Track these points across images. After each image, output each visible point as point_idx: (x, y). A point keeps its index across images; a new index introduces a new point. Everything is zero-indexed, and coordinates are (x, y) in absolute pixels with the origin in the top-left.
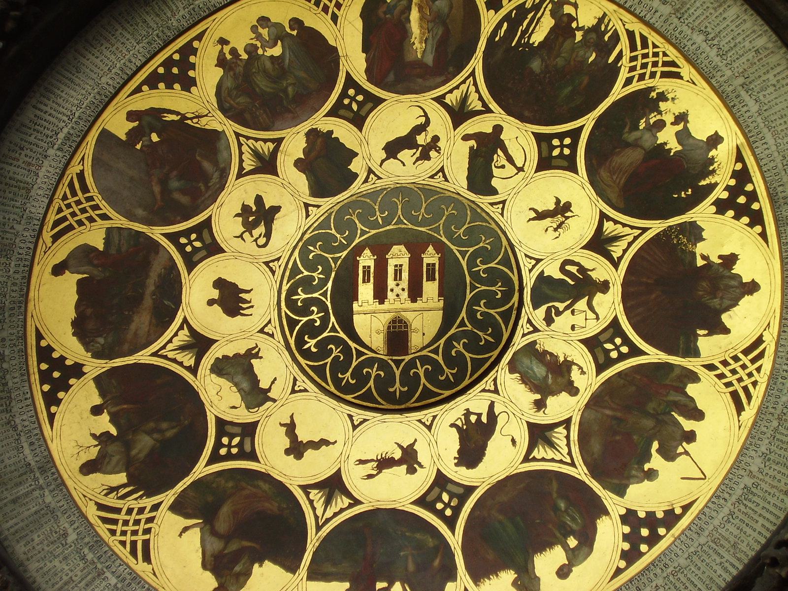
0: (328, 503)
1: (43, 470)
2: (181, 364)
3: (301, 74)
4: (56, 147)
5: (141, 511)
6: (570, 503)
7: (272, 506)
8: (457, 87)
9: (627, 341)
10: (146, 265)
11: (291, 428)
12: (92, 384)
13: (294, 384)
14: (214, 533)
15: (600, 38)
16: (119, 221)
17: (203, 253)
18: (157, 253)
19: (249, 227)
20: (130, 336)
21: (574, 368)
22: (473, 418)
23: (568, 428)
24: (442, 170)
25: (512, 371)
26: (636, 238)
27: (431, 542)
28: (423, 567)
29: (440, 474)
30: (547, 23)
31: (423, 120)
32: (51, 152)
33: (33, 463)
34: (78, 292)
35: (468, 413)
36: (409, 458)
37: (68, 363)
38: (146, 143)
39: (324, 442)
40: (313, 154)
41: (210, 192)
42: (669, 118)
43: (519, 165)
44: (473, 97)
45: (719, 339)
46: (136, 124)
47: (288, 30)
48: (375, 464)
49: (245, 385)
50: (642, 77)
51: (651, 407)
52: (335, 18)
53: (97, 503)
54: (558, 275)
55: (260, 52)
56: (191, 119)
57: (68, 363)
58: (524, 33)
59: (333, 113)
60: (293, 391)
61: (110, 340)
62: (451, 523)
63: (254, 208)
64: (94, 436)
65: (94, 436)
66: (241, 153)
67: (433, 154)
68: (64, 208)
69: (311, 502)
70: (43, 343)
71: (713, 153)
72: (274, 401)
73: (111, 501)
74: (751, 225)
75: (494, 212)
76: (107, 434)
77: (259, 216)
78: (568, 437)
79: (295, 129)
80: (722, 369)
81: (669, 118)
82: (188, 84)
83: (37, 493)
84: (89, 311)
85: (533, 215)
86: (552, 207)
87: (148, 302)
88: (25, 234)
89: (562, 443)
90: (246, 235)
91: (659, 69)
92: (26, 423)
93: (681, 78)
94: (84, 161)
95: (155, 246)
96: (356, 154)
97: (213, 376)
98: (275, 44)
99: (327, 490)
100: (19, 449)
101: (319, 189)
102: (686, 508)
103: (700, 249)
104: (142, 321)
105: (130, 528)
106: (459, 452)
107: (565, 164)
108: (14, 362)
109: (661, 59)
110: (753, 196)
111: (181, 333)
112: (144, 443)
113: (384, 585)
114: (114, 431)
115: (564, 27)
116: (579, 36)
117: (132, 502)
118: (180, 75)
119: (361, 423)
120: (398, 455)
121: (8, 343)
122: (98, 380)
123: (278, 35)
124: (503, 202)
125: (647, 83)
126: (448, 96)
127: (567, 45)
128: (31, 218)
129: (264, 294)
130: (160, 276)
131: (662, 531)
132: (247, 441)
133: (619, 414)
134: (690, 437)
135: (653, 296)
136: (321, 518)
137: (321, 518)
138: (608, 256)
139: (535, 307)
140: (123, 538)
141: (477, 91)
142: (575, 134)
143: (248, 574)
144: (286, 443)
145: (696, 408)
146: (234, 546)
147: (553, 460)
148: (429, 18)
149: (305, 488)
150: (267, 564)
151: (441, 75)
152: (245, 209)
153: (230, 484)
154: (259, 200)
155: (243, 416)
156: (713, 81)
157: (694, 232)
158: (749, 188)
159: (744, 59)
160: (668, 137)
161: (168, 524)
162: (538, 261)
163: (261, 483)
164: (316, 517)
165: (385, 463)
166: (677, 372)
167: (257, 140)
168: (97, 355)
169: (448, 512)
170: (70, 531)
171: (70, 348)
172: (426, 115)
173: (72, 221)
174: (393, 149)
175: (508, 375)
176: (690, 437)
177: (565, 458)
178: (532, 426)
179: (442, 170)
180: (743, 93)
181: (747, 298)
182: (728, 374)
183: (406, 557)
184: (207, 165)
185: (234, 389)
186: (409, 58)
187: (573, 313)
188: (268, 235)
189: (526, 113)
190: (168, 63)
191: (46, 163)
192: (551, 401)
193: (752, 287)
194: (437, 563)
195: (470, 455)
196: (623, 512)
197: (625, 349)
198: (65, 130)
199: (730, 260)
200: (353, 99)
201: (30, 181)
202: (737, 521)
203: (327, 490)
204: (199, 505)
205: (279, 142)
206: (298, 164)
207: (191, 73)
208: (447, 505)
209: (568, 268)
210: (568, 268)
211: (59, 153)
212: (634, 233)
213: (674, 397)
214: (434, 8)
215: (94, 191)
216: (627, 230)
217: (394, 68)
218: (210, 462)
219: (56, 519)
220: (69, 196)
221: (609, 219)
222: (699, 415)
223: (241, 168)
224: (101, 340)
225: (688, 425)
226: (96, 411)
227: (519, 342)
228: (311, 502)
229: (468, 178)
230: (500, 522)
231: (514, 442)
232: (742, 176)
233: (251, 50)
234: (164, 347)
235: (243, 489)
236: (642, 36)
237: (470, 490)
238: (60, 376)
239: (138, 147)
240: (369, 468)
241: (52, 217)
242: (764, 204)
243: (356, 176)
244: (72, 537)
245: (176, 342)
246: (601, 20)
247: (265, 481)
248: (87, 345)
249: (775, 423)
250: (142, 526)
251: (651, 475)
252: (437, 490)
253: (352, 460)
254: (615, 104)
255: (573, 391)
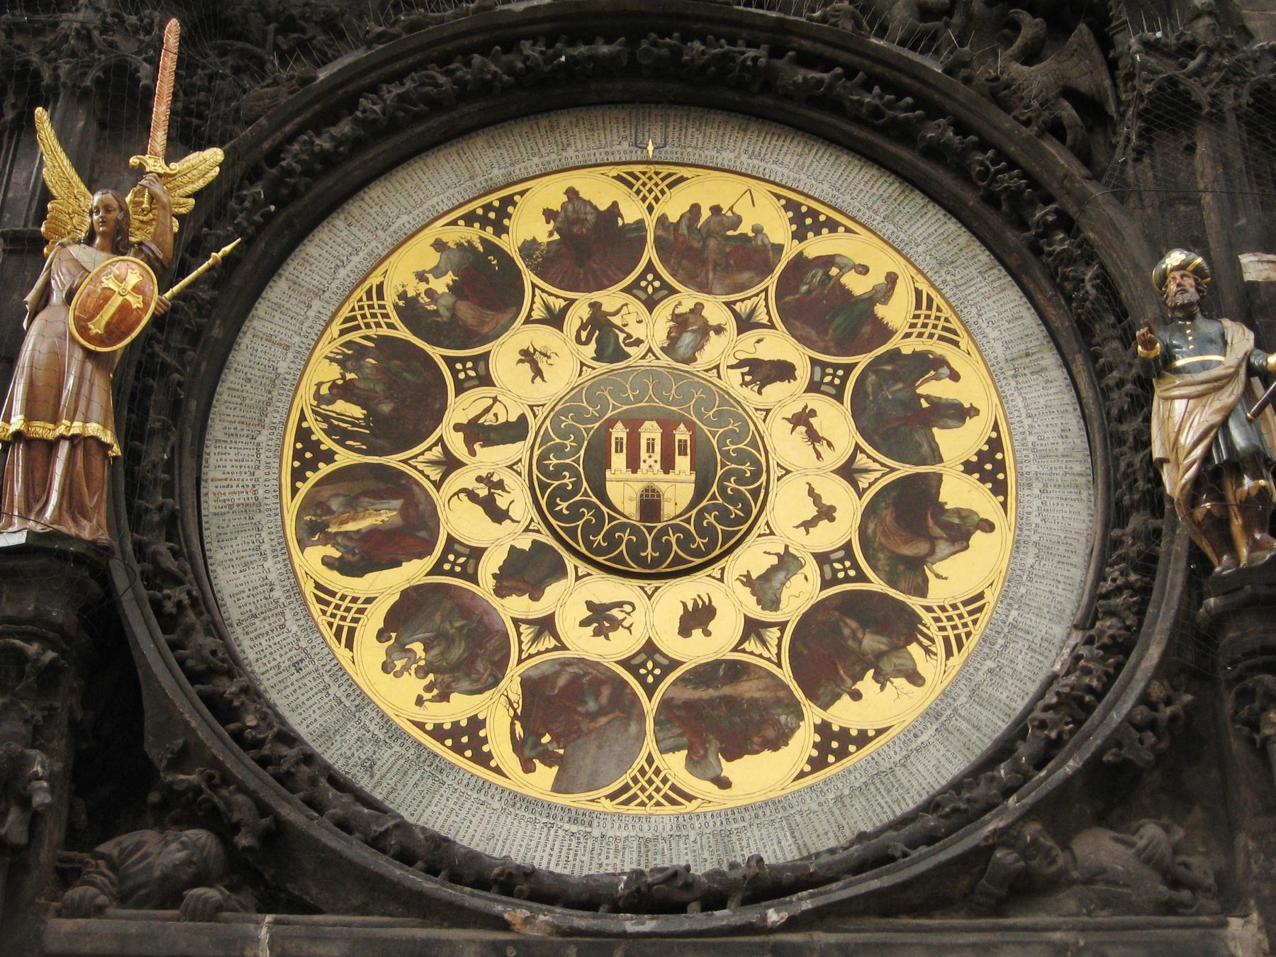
0: (867, 471)
1: (938, 716)
2: (780, 639)
3: (438, 618)
4: (589, 830)
5: (937, 620)
6: (802, 282)
7: (888, 515)
8: (422, 472)
9: (642, 276)
10: (688, 705)
11: (808, 525)
12: (832, 710)
13: (764, 535)
14: (932, 552)
15: (351, 357)
16: (650, 745)
17: (658, 657)
18: (672, 699)
19: (616, 624)
20: (769, 695)
21: (677, 312)
22: (748, 378)
23: (735, 302)
24: (511, 467)
25: (695, 360)
26: (543, 291)
27: (872, 378)
28: (895, 377)
29: (807, 391)
30: (341, 406)
31: (462, 495)
32: (596, 832)
33: (935, 727)
34: (740, 756)
35: (744, 384)
36: (802, 419)
37: (818, 739)
38: (555, 745)
39: (811, 492)
40: (522, 586)
41: (590, 670)
42: (423, 287)
43: (491, 401)
44: (428, 456)
45: (623, 209)
46: (536, 761)
47: (392, 642)
48: (817, 445)
49: (781, 576)
50: (385, 316)
51: (696, 245)
52: (369, 601)
53: (947, 658)
54: (593, 345)
55: (422, 663)
56: (515, 710)
57: (818, 739)
58: (353, 424)
59: (474, 579)
60: (772, 533)
61: (780, 711)
62: (849, 368)
63: (595, 625)
64: (882, 689)
65: (882, 689)
66: (539, 653)
67: (495, 478)
68: (654, 801)
69: (871, 485)
70: (808, 768)
71: (452, 245)
72: (787, 547)
73: (939, 647)
74: (515, 204)
75: (542, 414)
76: (875, 678)
77: (601, 618)
78: (742, 301)
79: (500, 610)
80: (650, 199)
81: (423, 287)
82: (476, 724)
83: (963, 712)
84: (756, 740)
85: (538, 379)
86: (527, 365)
87: (727, 690)
88: (697, 825)
89: (749, 303)
90: (626, 624)
91: (375, 302)
92: (897, 749)
93: (382, 283)
94: (593, 801)
95: (665, 704)
96: (512, 547)
97: (781, 606)
98: (411, 650)
99: (856, 476)
100: (925, 745)
101: (558, 571)
102: (779, 197)
103: (543, 238)
104: (748, 689)
105: (957, 621)
106: (782, 380)
107: (482, 364)
108: (840, 785)
109: (365, 303)
110: (488, 207)
111: (748, 649)
112: (871, 642)
113: (923, 401)
114: (871, 672)
115: (343, 391)
116: (350, 376)
117: (933, 631)
118: (468, 737)
119: (782, 468)
120: (802, 429)
121: (822, 799)
122: (825, 707)
123: (401, 648)
124: (531, 407)
125: (390, 310)
126: (432, 478)
127: (361, 385)
128: (678, 826)
129: (679, 594)
130: (695, 689)
131: (804, 209)
132: (833, 556)
133: (711, 267)
134: (716, 210)
135: (595, 266)
136: (882, 471)
137: (882, 471)
138: (565, 310)
139: (627, 356)
140: (970, 624)
141: (422, 453)
142: (450, 361)
143: (958, 511)
144: (824, 524)
145: (690, 211)
146: (937, 531)
147: (767, 306)
148: (352, 513)
149: (860, 494)
150: (941, 499)
151: (411, 490)
152: (597, 633)
153: (881, 556)
154: (585, 623)
155: (812, 568)
156: (383, 254)
157: (528, 248)
158: (480, 212)
159: (359, 234)
160: (441, 285)
161: (938, 592)
162: (582, 364)
163: (870, 531)
164: (883, 475)
165: (814, 437)
166: (660, 232)
167: (520, 642)
168: (800, 716)
169: (840, 373)
170: (985, 668)
171: (803, 742)
172: (457, 494)
173: (665, 789)
174: (498, 515)
175: (699, 360)
176: (716, 210)
177: (761, 297)
178: (741, 330)
179: (511, 467)
180: (392, 229)
181: (582, 195)
182: (653, 195)
183: (892, 393)
184: (562, 681)
185: (788, 584)
186: (398, 521)
187: (625, 325)
188: (619, 605)
189: (437, 406)
190: (458, 749)
191: (610, 833)
192: (713, 322)
193: (572, 193)
194: (888, 368)
195: (783, 371)
196: (796, 242)
197: (650, 277)
198: (566, 826)
199: (549, 215)
200: (454, 564)
201: (635, 843)
202: (780, 158)
203: (856, 476)
204: (912, 573)
205: (516, 622)
206: (535, 597)
207: (464, 723)
208: (834, 376)
209: (583, 339)
210: (583, 339)
211: (595, 824)
212: (538, 293)
213: (684, 229)
214: (341, 510)
215: (626, 779)
216: (537, 299)
217: (415, 532)
218: (867, 580)
219: (978, 686)
220: (639, 801)
221: (529, 315)
222: (695, 209)
223: (555, 649)
224: (783, 718)
225: (706, 214)
226: (856, 696)
227: (665, 360)
228: (871, 485)
229: (513, 442)
230: (835, 330)
231: (759, 341)
232: (470, 219)
233: (422, 672)
234: (769, 660)
235: (881, 544)
236: (344, 323)
237: (814, 362)
238: (834, 743)
239: (561, 751)
240: (822, 448)
241: (669, 809)
242: (494, 199)
243: (534, 542)
244: (990, 664)
245: (759, 649)
246: (332, 360)
247: (866, 528)
248: (792, 731)
249: (689, 150)
250: (951, 612)
251: (758, 230)
252: (823, 388)
253: (819, 464)
254: (415, 334)
255: (699, 307)
